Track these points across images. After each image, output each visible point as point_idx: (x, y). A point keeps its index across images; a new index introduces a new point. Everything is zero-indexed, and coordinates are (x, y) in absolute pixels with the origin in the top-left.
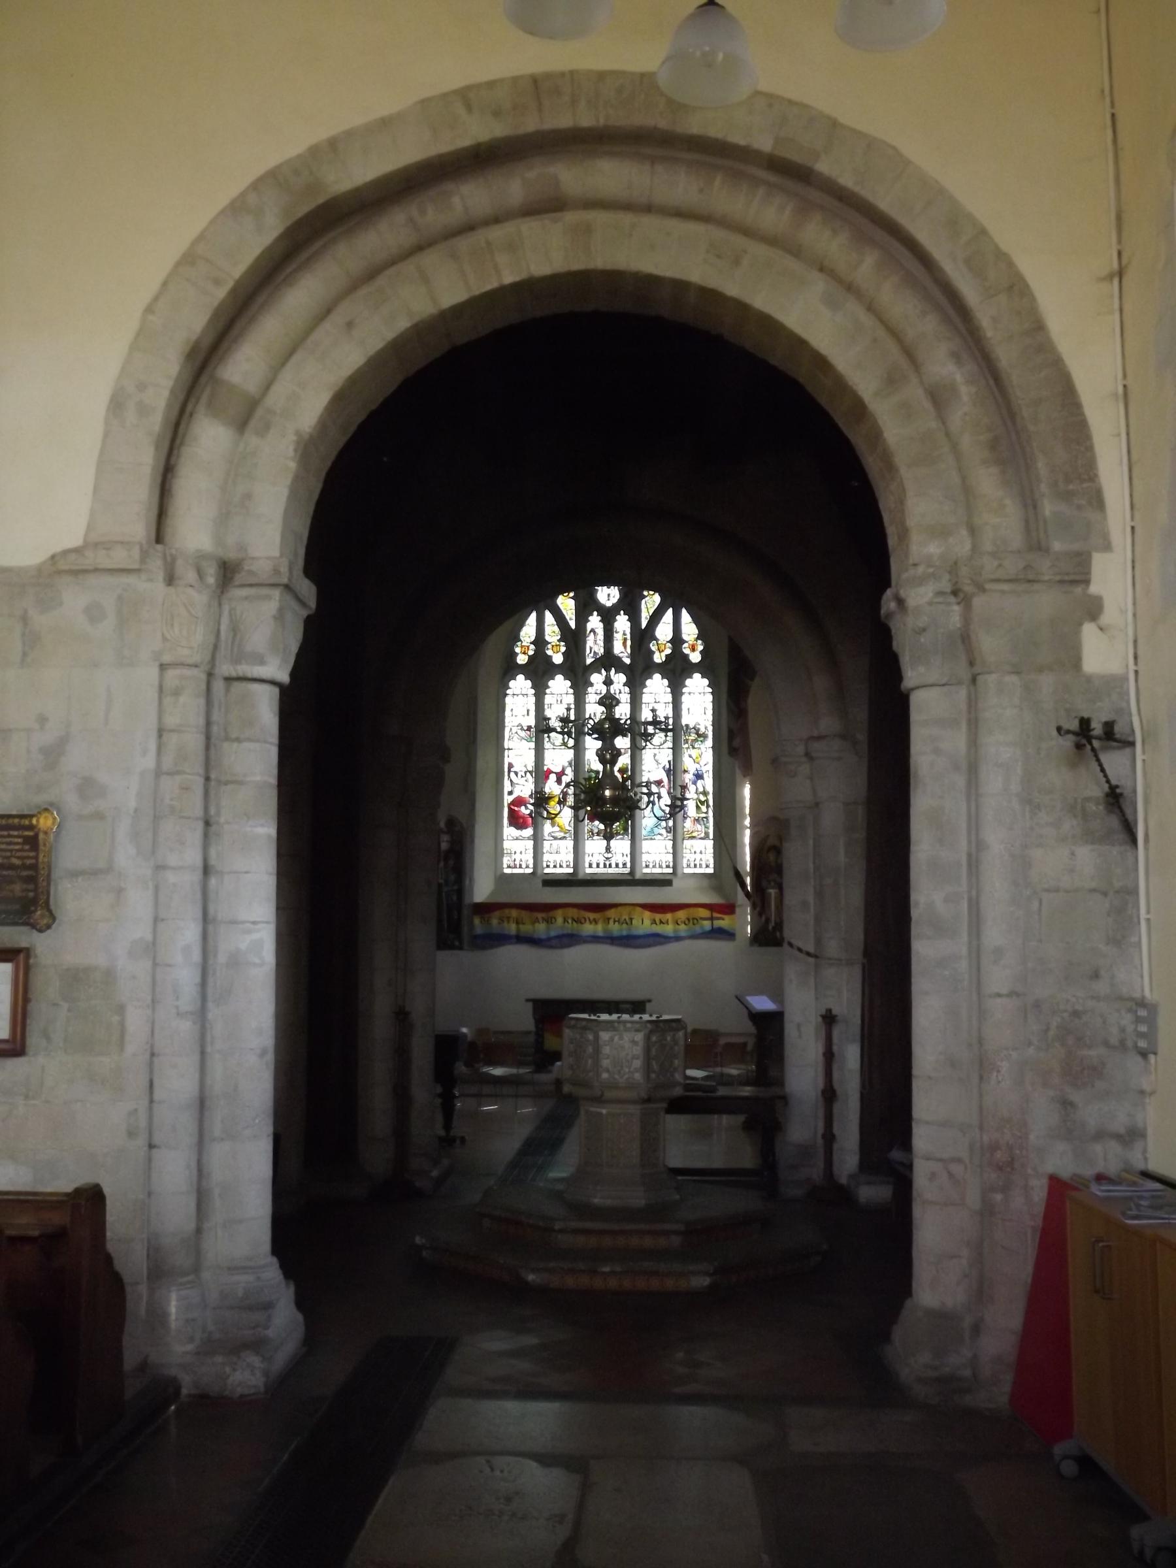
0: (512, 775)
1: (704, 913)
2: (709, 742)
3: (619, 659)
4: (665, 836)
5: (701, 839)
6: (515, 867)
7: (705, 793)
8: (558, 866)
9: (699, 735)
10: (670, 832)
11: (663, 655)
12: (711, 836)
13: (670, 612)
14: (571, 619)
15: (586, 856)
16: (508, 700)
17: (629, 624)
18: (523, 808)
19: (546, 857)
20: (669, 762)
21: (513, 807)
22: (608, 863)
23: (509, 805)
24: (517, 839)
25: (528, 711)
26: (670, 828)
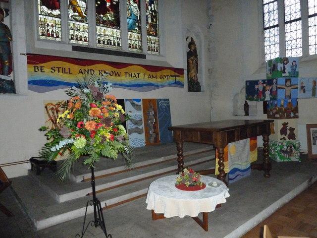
1: (173, 73)
6: (49, 35)
7: (155, 11)
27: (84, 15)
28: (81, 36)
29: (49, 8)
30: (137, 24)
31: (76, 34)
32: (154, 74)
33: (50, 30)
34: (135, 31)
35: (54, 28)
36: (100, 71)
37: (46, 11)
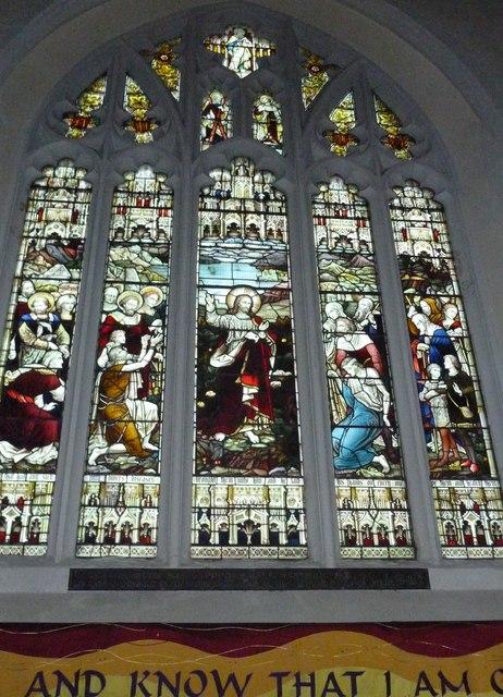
0: (24, 328)
7: (462, 379)
8: (118, 539)
18: (39, 401)
22: (248, 532)
25: (76, 214)
27: (147, 445)
29: (18, 444)
30: (379, 441)
31: (106, 520)
32: (452, 667)
34: (373, 472)
35: (26, 509)
36: (134, 675)
37: (8, 456)
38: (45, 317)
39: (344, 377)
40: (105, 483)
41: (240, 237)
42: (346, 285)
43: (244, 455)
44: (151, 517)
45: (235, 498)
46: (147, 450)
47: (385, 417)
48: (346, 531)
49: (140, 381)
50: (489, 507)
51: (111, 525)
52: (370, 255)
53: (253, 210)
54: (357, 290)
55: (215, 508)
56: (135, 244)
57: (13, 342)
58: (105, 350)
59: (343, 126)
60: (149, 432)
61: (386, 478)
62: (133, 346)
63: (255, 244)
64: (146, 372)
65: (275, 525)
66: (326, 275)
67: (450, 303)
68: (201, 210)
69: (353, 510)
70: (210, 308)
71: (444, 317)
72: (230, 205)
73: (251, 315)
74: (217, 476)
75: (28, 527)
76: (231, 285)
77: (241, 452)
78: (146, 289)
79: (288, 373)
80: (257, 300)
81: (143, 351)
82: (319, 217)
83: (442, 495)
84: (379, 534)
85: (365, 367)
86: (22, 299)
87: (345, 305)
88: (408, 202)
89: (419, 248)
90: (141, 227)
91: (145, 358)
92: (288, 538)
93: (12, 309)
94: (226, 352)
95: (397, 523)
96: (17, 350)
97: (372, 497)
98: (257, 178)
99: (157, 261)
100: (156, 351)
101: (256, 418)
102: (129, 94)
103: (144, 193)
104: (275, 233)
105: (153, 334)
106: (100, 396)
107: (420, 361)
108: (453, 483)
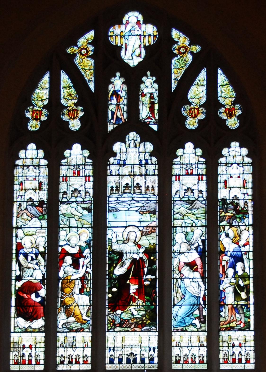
0: (21, 258)
2: (249, 220)
3: (146, 125)
4: (198, 327)
5: (240, 330)
6: (24, 363)
7: (245, 277)
9: (238, 212)
10: (203, 322)
11: (196, 120)
12: (252, 328)
13: (203, 75)
14: (90, 80)
15: (107, 351)
16: (18, 171)
17: (156, 86)
18: (33, 296)
19: (60, 352)
20: (203, 241)
21: (22, 295)
22: (131, 358)
23: (17, 292)
24: (26, 331)
25: (40, 184)
26: (204, 317)
27: (85, 318)
28: (78, 355)
29: (27, 319)
30: (197, 312)
31: (68, 353)
33: (27, 354)
34: (192, 328)
35: (33, 349)
38: (31, 250)
39: (182, 278)
40: (67, 336)
41: (130, 193)
42: (188, 221)
43: (130, 321)
44: (88, 352)
45: (126, 342)
46: (85, 320)
47: (201, 300)
48: (176, 357)
49: (80, 284)
50: (246, 345)
51: (70, 356)
52: (204, 200)
53: (138, 173)
54: (194, 225)
55: (116, 347)
56: (73, 202)
57: (17, 265)
58: (62, 268)
59: (196, 101)
60: (86, 310)
61: (198, 331)
62: (76, 265)
63: (138, 197)
64: (83, 279)
65: (143, 355)
66: (177, 216)
67: (245, 230)
68: (109, 175)
69: (180, 347)
70: (114, 240)
71: (240, 239)
72: (126, 170)
73: (136, 244)
74: (117, 332)
75: (35, 357)
76: (125, 226)
77: (128, 320)
78: (81, 230)
79: (154, 277)
80: (139, 234)
81: (81, 267)
82: (176, 175)
83: (224, 339)
84: (191, 358)
85: (194, 271)
86: (19, 241)
87: (187, 234)
88: (230, 160)
89: (235, 192)
90: (76, 190)
91: (82, 271)
92: (150, 360)
93: (14, 247)
94: (122, 266)
95: (200, 353)
96: (20, 270)
97: (190, 340)
98: (142, 149)
99: (86, 212)
100: (87, 267)
101: (136, 302)
102: (63, 88)
103: (77, 165)
104: (150, 189)
105: (85, 257)
106: (61, 293)
107: (223, 267)
108: (230, 333)
